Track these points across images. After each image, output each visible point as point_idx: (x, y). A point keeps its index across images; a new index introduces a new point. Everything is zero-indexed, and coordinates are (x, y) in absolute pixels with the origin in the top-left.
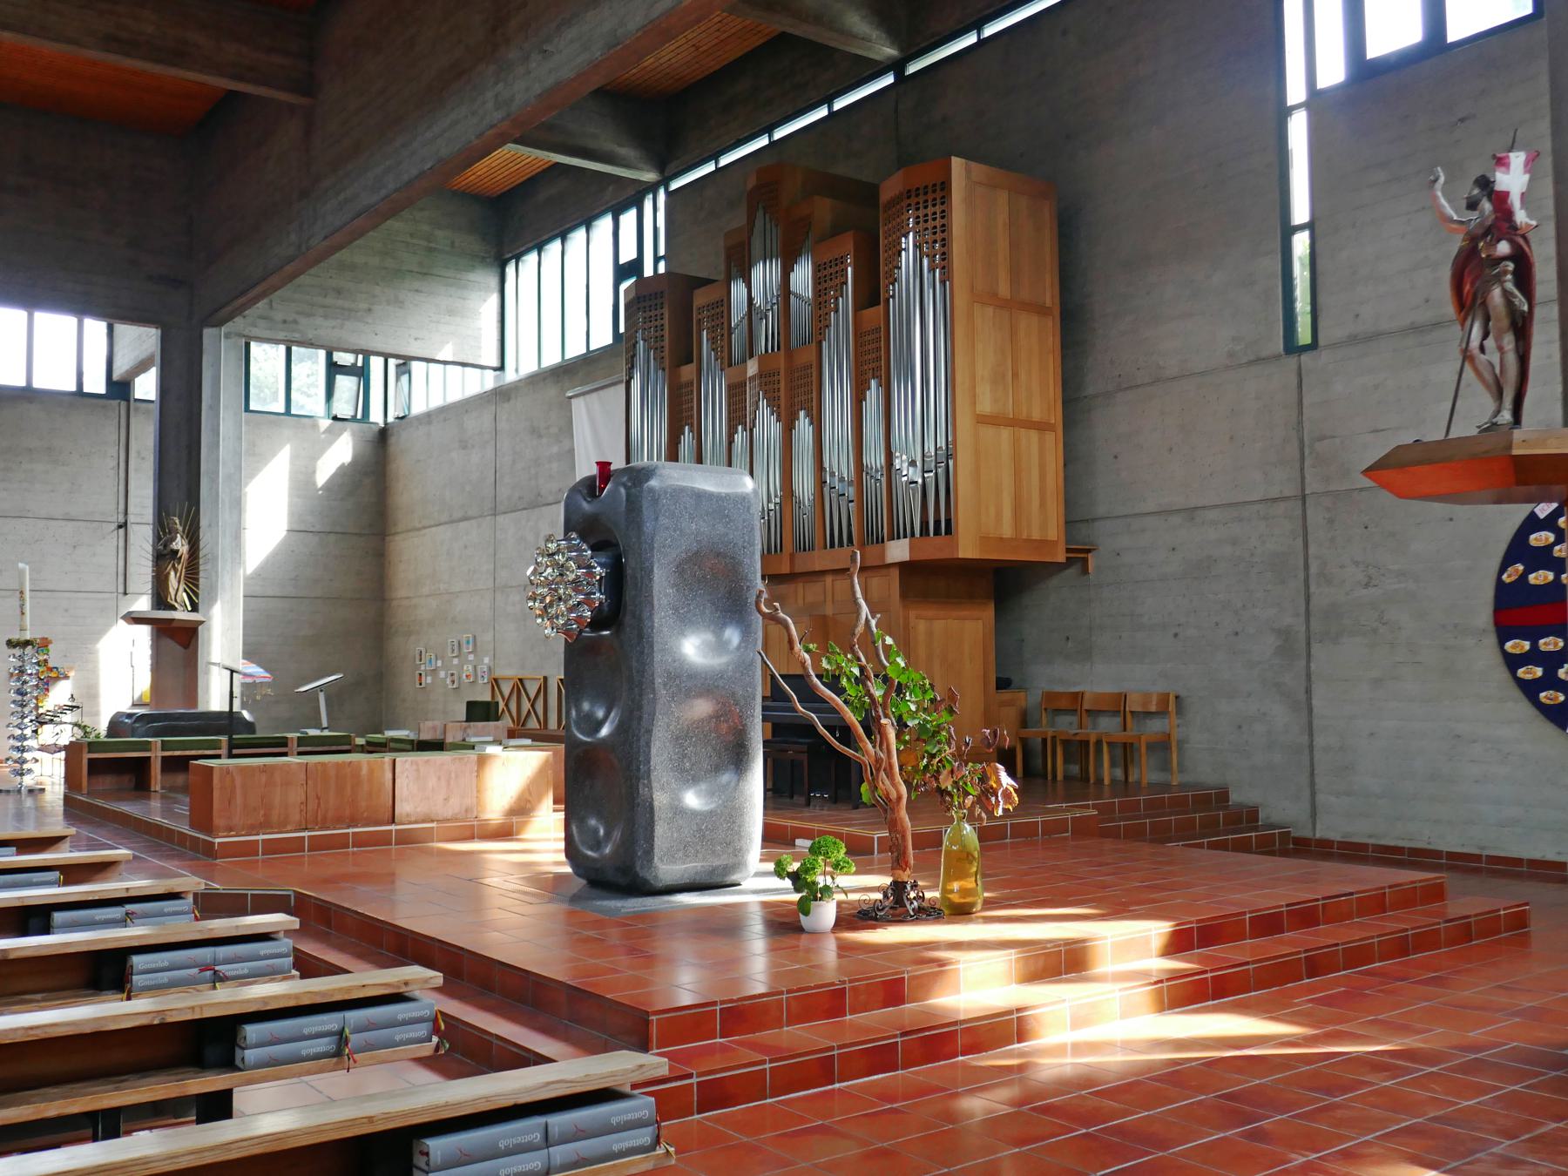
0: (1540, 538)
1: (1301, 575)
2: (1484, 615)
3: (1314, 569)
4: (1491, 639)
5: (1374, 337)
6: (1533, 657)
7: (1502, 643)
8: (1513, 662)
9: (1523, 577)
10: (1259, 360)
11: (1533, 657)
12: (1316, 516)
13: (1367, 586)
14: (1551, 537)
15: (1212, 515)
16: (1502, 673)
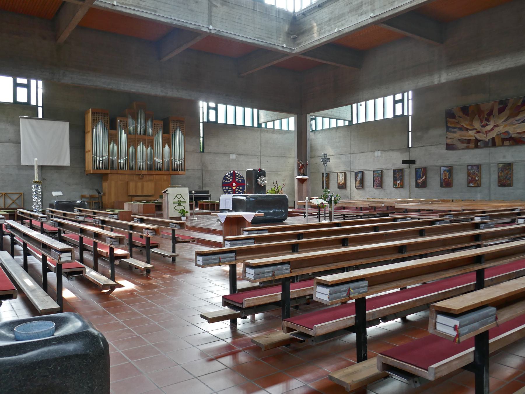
0: (227, 177)
1: (202, 179)
2: (221, 185)
3: (203, 179)
4: (222, 187)
5: (210, 153)
6: (226, 189)
7: (223, 188)
8: (224, 190)
9: (225, 181)
10: (197, 152)
11: (226, 189)
12: (204, 172)
13: (209, 181)
14: (227, 177)
15: (190, 170)
16: (222, 191)
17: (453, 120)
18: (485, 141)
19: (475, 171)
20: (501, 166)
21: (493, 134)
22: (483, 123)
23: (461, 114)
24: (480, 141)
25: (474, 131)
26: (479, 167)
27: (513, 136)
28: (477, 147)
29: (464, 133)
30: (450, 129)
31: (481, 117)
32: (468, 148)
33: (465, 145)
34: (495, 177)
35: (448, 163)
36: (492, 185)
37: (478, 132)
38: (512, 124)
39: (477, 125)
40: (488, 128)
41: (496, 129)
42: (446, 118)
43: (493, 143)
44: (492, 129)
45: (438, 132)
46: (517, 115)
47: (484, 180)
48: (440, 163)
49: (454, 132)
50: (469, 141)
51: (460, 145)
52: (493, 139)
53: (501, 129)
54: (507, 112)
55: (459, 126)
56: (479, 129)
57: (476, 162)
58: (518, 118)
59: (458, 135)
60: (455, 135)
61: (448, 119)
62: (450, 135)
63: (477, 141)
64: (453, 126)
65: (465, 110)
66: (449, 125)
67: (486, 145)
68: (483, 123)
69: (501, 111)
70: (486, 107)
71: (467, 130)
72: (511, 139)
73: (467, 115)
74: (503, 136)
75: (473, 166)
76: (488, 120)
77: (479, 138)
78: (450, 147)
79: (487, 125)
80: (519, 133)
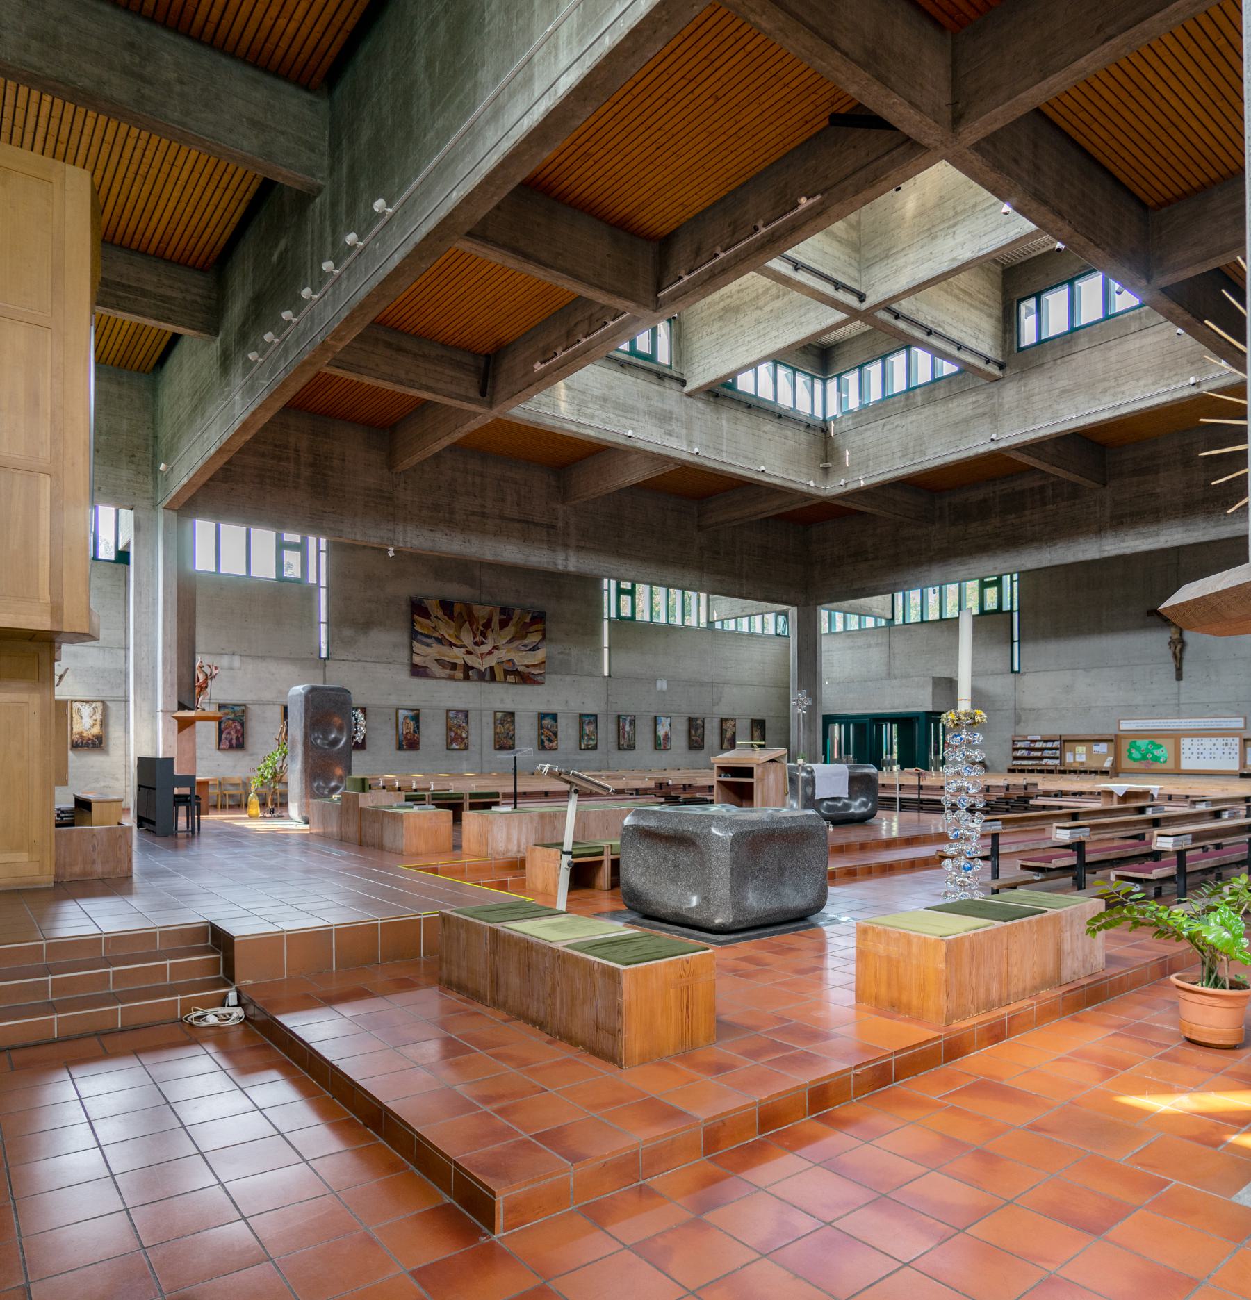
17: (426, 621)
18: (479, 671)
19: (460, 720)
20: (499, 715)
21: (491, 661)
22: (477, 639)
23: (440, 613)
24: (472, 668)
25: (463, 650)
26: (466, 714)
27: (520, 669)
28: (467, 678)
29: (446, 649)
30: (420, 637)
31: (474, 627)
32: (451, 678)
33: (448, 671)
34: (489, 733)
35: (410, 703)
36: (485, 749)
37: (469, 653)
38: (517, 649)
39: (467, 638)
40: (485, 649)
41: (496, 652)
42: (413, 614)
43: (489, 676)
44: (490, 652)
45: (391, 640)
46: (524, 637)
47: (473, 739)
48: (393, 700)
49: (428, 645)
50: (454, 666)
51: (437, 670)
52: (492, 668)
53: (503, 654)
54: (510, 630)
55: (436, 635)
56: (470, 648)
57: (460, 705)
58: (526, 642)
59: (435, 651)
60: (429, 650)
61: (416, 617)
62: (418, 647)
63: (467, 668)
64: (425, 631)
65: (447, 607)
66: (418, 628)
67: (481, 677)
68: (477, 639)
69: (503, 624)
70: (481, 612)
71: (451, 645)
72: (516, 673)
73: (451, 617)
74: (506, 666)
75: (458, 711)
76: (484, 635)
77: (470, 664)
78: (418, 671)
79: (483, 643)
80: (527, 666)
